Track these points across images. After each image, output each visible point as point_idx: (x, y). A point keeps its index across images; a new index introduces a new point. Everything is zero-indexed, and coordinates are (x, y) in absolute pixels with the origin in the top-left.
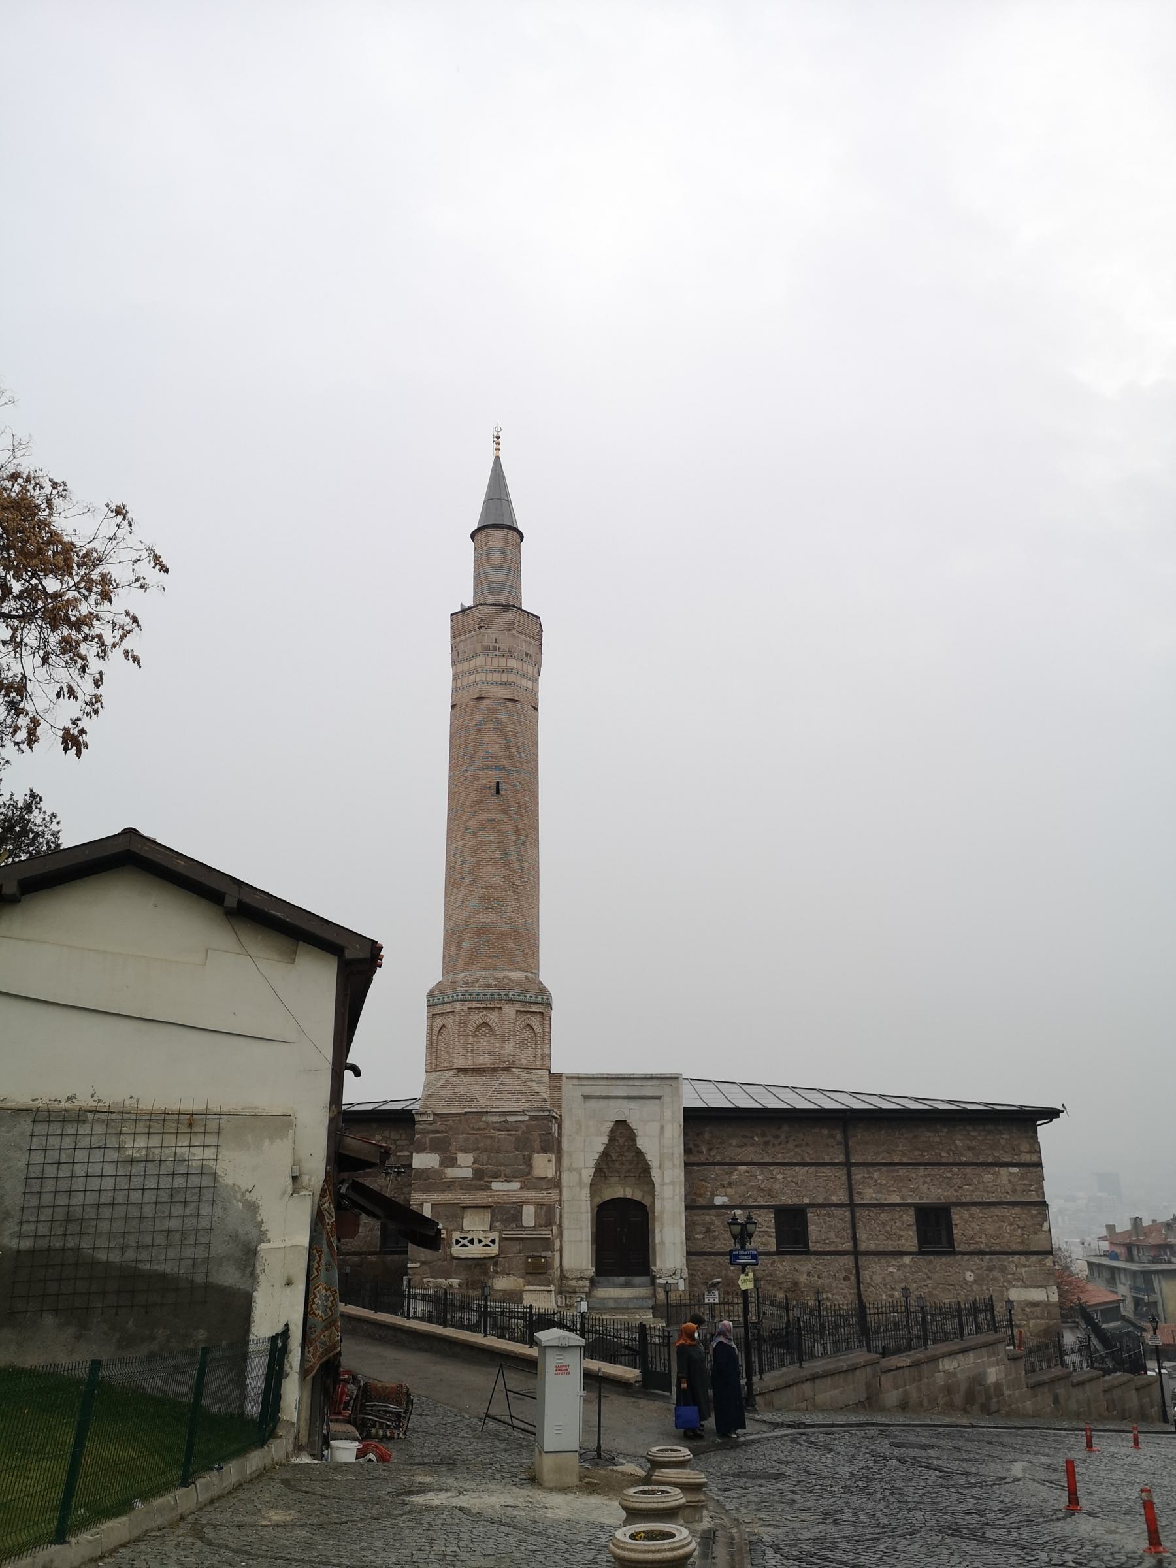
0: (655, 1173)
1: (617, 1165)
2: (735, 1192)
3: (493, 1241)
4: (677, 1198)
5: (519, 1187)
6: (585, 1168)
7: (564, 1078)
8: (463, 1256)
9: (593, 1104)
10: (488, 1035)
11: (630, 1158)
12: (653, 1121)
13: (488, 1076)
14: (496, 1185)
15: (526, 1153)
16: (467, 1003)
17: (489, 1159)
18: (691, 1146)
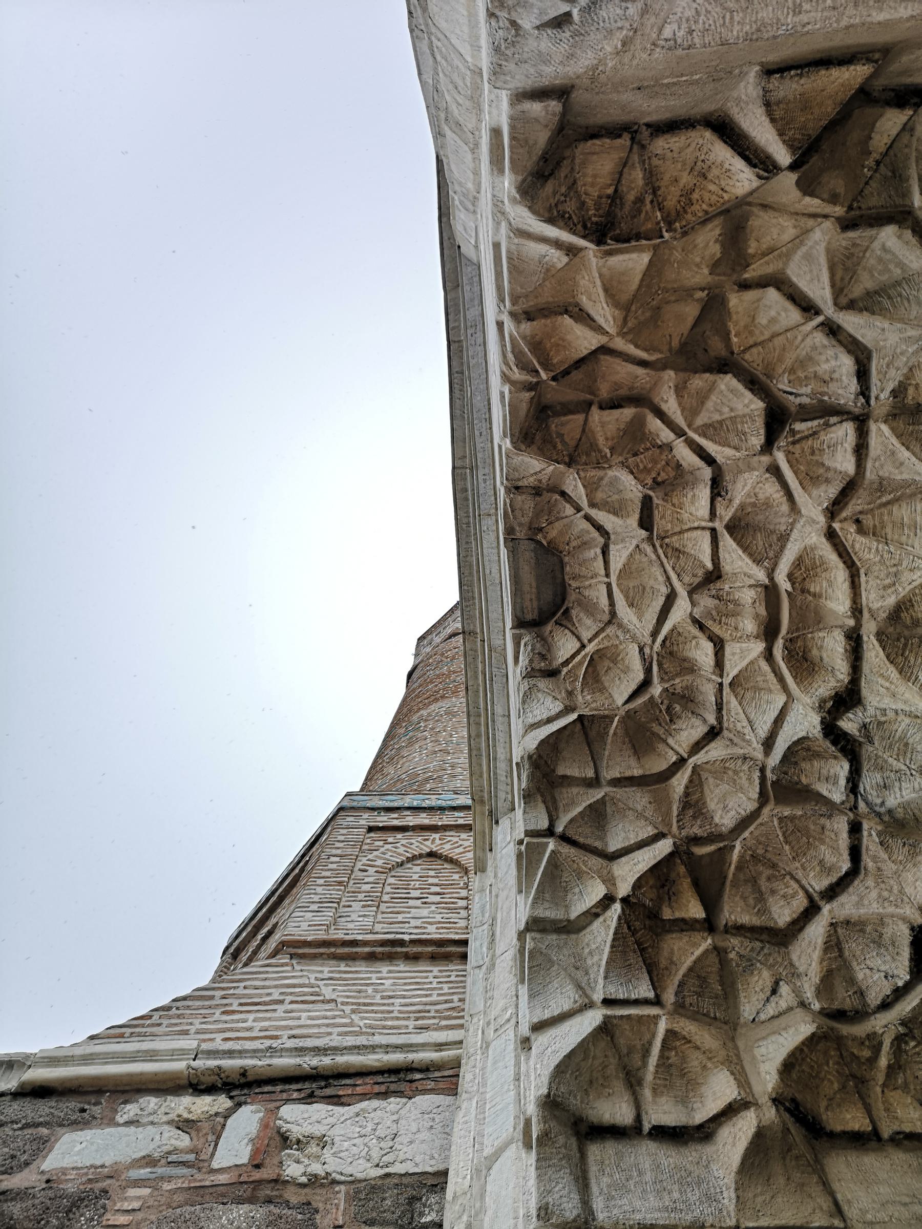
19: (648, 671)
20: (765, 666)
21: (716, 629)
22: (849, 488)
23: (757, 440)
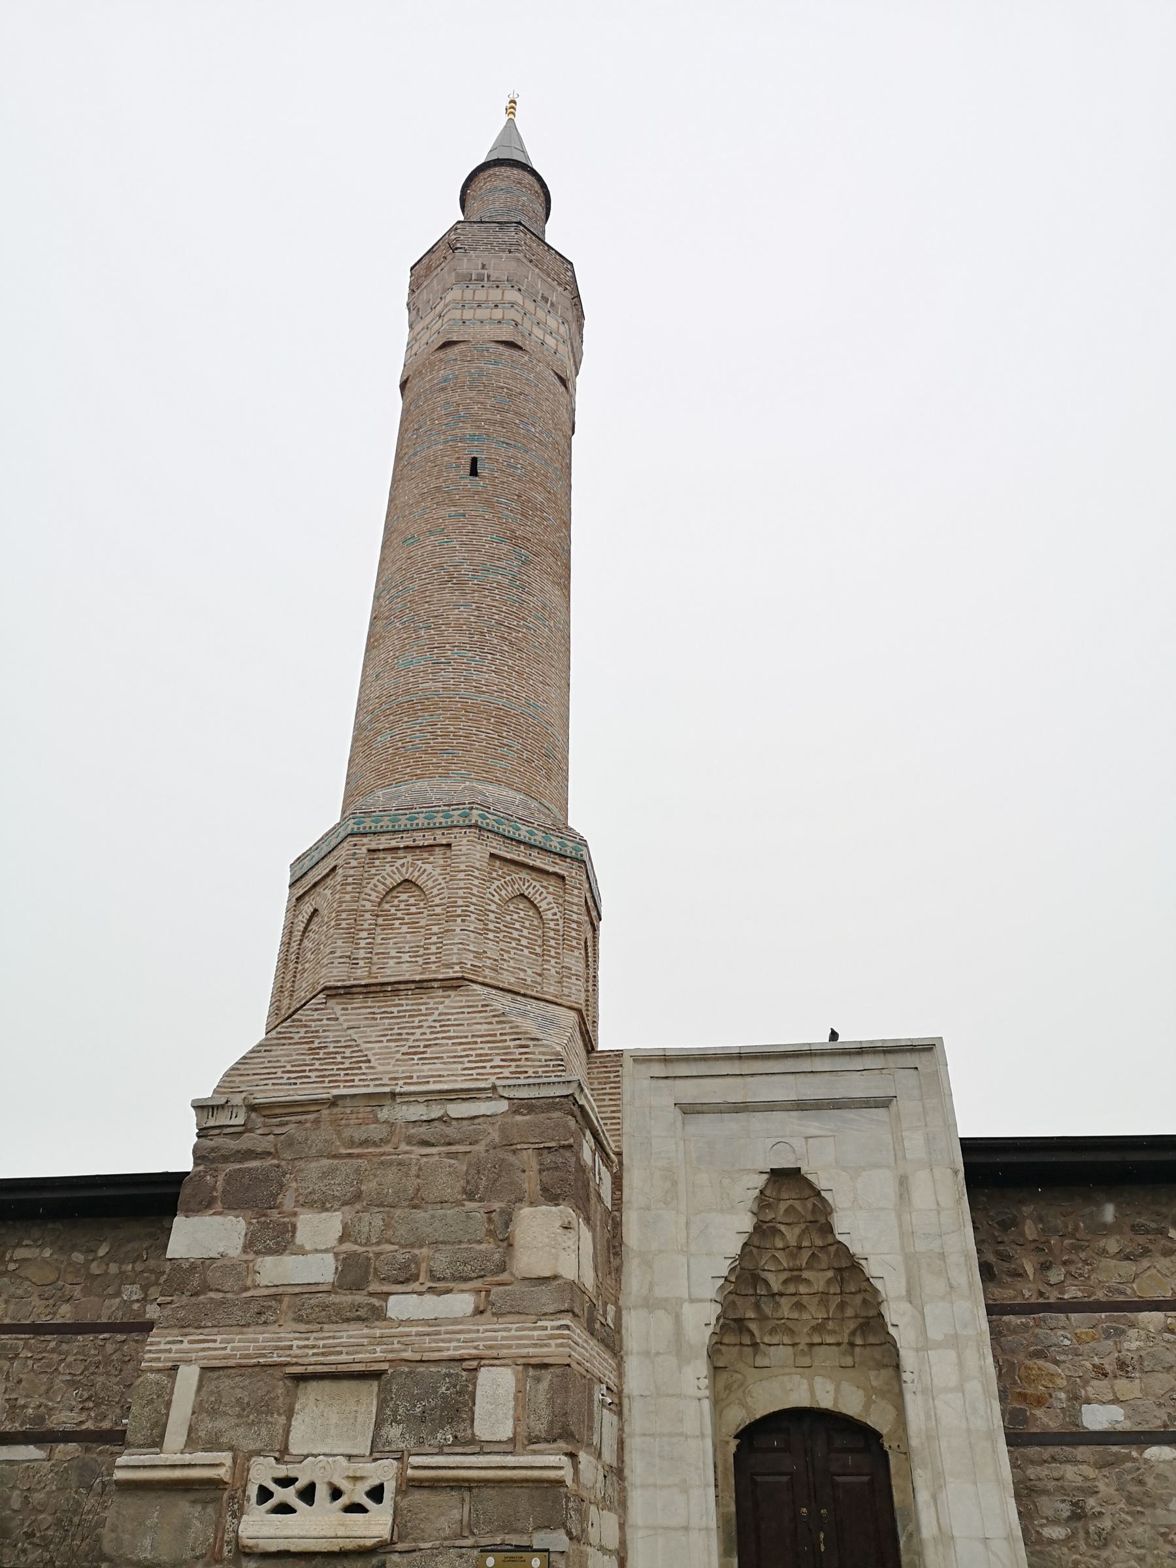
0: (896, 1314)
1: (786, 1307)
2: (1145, 1392)
3: (376, 1494)
4: (974, 1387)
5: (470, 1309)
6: (692, 1301)
7: (628, 1062)
8: (273, 1547)
9: (706, 1125)
10: (413, 909)
11: (819, 1286)
12: (875, 1166)
13: (406, 1003)
14: (401, 1306)
15: (497, 1206)
16: (365, 840)
17: (387, 1226)
18: (991, 1258)
19: (769, 1222)
20: (782, 1268)
21: (787, 1250)
22: (828, 1294)
23: (836, 1265)
